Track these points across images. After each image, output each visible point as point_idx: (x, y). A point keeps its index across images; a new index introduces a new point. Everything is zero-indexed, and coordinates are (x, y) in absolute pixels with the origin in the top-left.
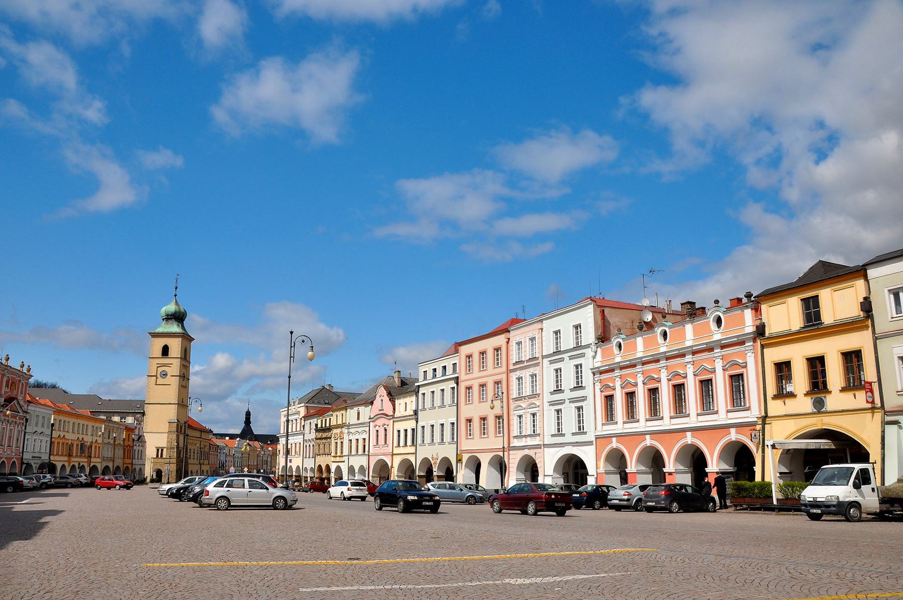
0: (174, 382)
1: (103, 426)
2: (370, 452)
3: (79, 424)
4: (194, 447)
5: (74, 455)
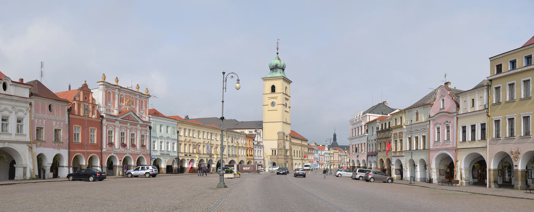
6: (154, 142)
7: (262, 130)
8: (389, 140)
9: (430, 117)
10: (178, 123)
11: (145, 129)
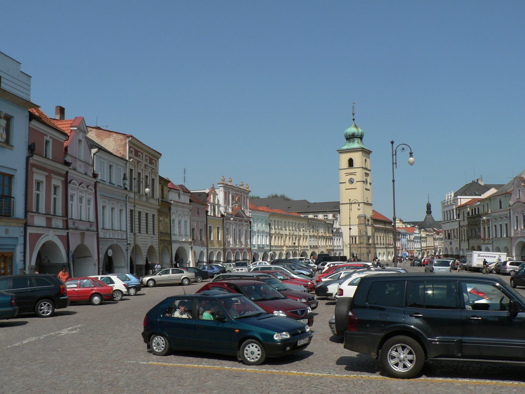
7: (339, 213)
9: (510, 206)
10: (269, 215)
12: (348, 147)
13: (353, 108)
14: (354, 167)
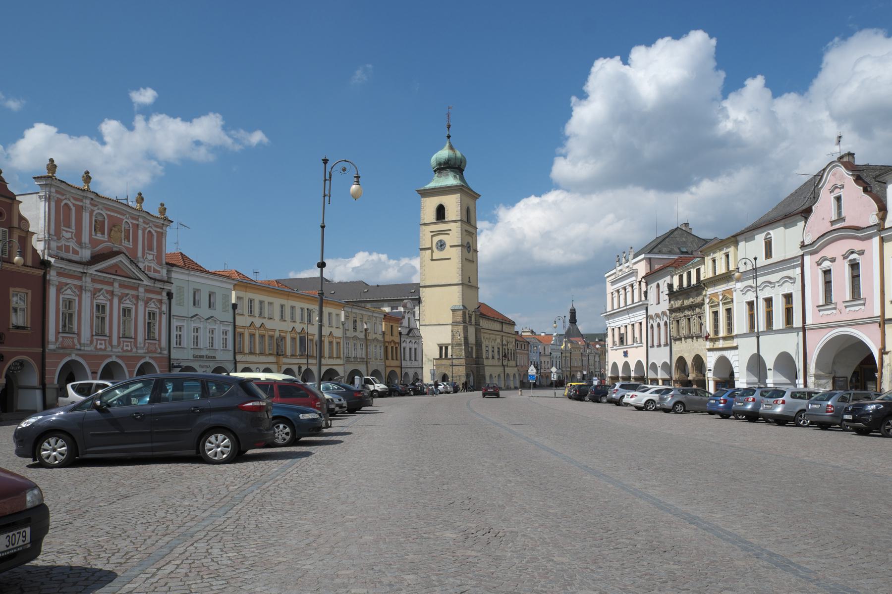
0: (455, 254)
1: (343, 312)
2: (809, 321)
3: (293, 308)
4: (491, 343)
5: (289, 352)
6: (180, 328)
8: (697, 310)
11: (159, 297)
12: (437, 185)
13: (448, 116)
14: (446, 220)
